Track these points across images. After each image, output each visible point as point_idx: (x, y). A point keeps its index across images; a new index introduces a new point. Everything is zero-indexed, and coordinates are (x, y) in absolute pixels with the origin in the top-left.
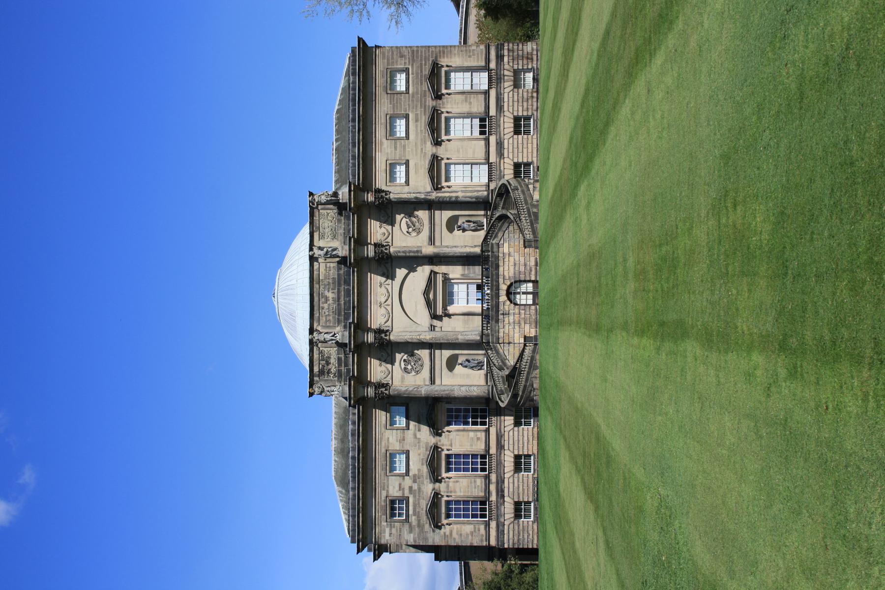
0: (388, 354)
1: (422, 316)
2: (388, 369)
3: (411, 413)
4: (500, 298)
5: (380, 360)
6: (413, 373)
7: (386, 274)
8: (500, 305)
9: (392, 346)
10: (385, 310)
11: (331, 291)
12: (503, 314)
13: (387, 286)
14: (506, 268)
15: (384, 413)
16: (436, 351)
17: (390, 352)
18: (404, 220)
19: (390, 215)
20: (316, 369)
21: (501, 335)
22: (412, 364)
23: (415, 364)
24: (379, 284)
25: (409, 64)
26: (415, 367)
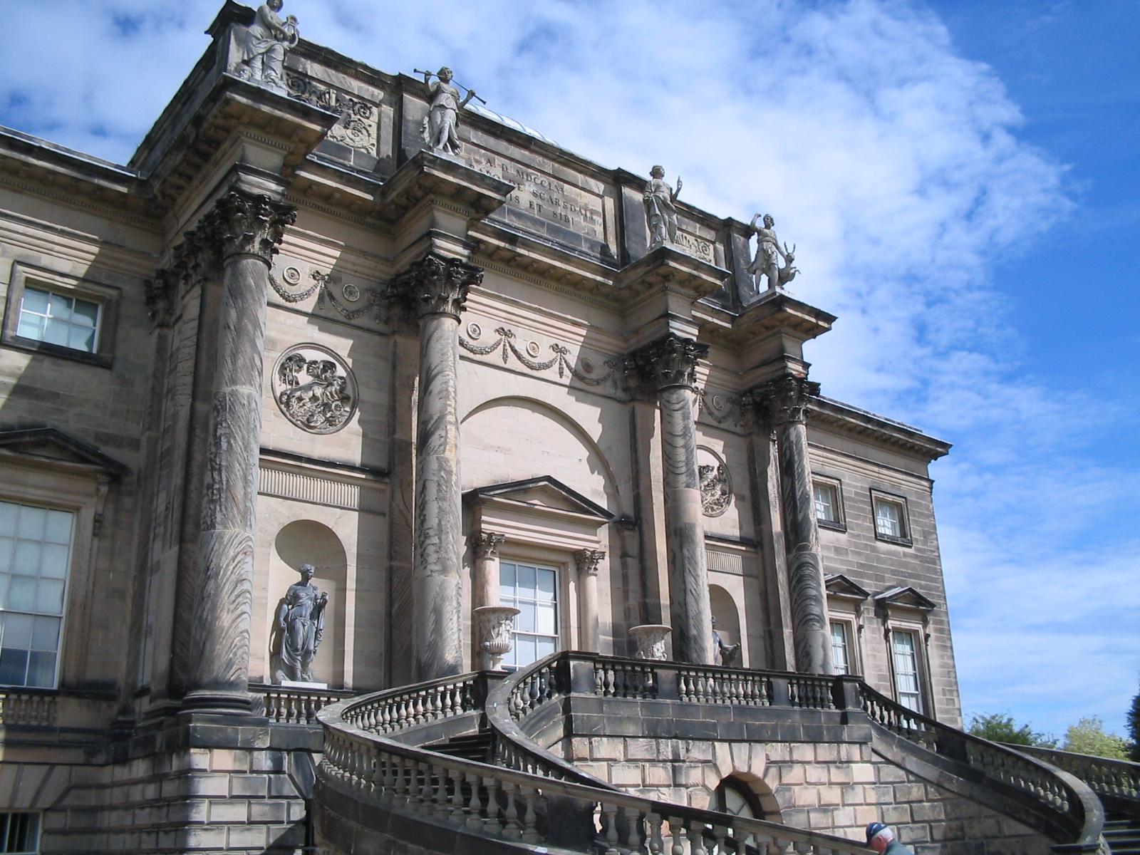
2: (302, 297)
3: (70, 371)
5: (332, 279)
6: (281, 388)
7: (586, 375)
8: (704, 745)
9: (381, 334)
11: (536, 201)
12: (676, 759)
14: (815, 773)
15: (81, 270)
16: (355, 491)
17: (358, 321)
18: (716, 464)
19: (723, 426)
20: (314, 69)
22: (318, 391)
23: (314, 398)
25: (917, 550)
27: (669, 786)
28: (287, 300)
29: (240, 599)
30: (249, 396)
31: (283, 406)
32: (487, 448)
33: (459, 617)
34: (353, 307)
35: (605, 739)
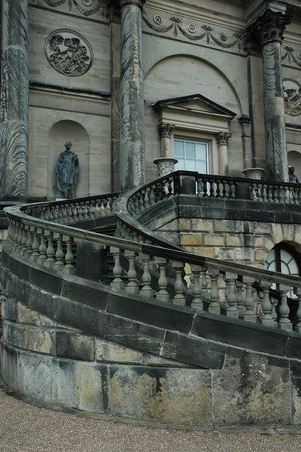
0: (90, 12)
1: (158, 89)
4: (279, 226)
8: (264, 225)
10: (168, 26)
12: (246, 232)
13: (205, 38)
21: (201, 225)
22: (70, 54)
24: (208, 25)
26: (64, 57)
27: (241, 247)
28: (51, 5)
29: (18, 155)
30: (18, 50)
31: (53, 63)
32: (166, 82)
33: (142, 163)
34: (88, 9)
35: (201, 220)
